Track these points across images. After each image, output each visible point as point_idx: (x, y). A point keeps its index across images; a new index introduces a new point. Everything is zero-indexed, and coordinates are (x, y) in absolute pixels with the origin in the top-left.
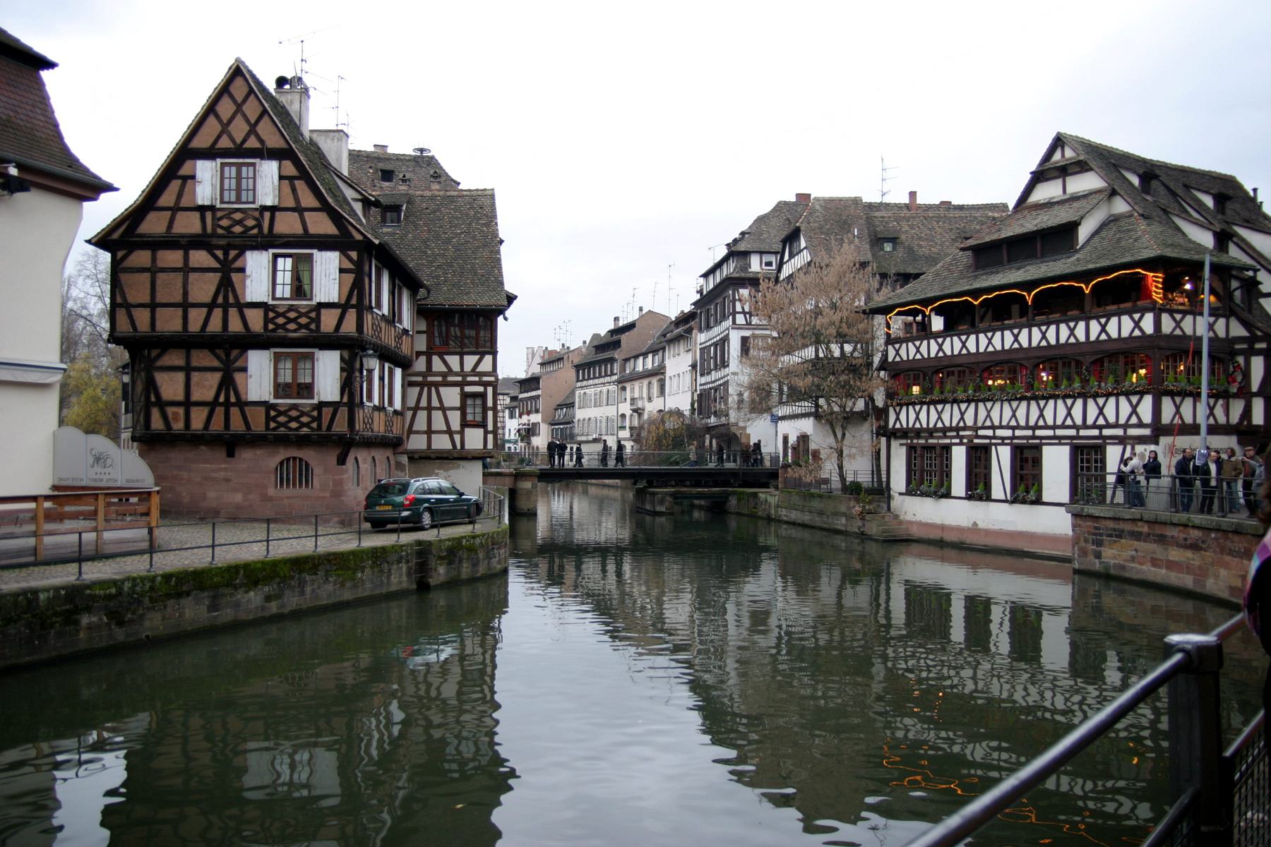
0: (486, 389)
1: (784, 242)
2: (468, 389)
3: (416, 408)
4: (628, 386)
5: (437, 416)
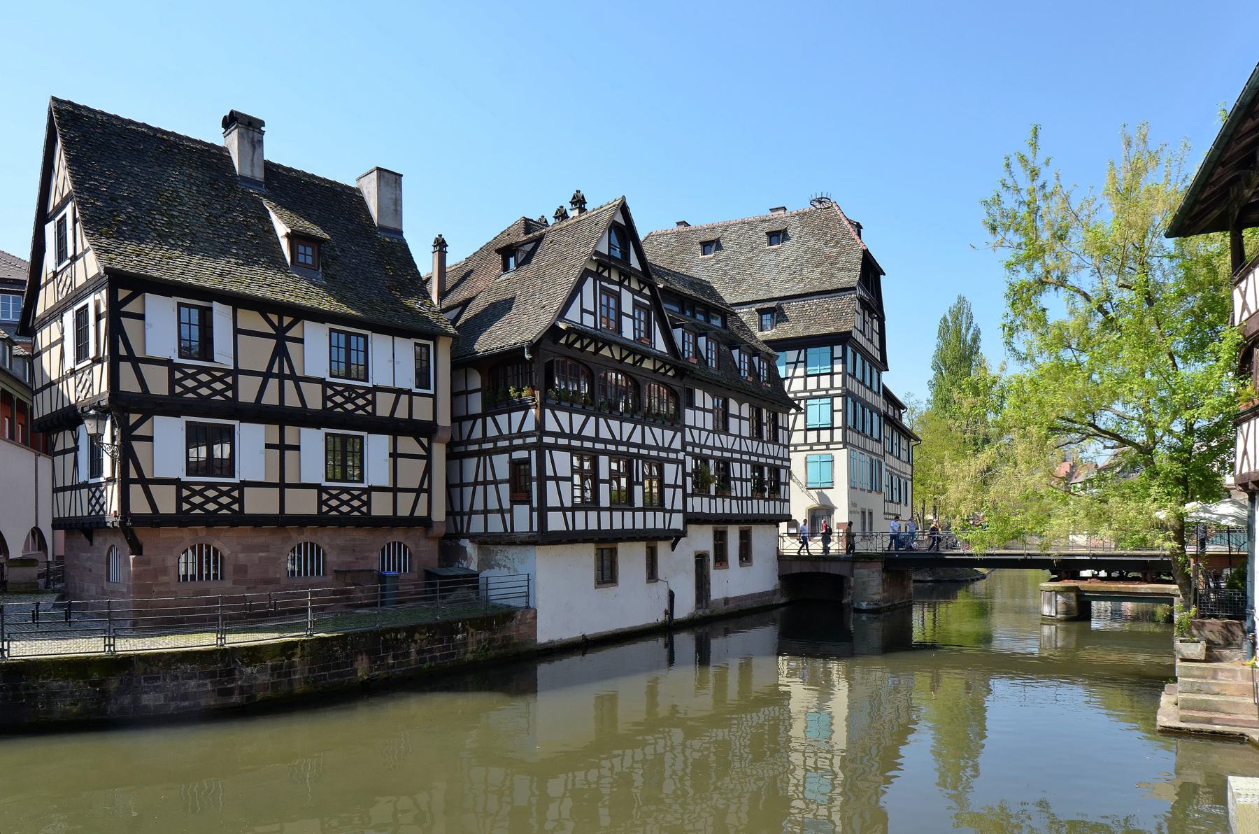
2: (517, 455)
3: (476, 483)
5: (491, 488)
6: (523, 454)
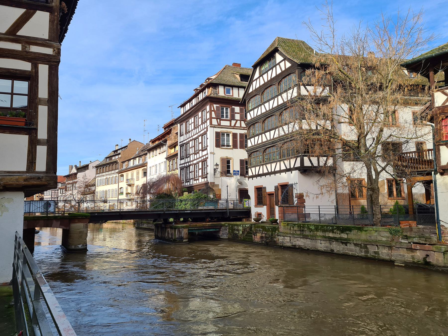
0: (35, 67)
1: (255, 67)
4: (125, 174)
6: (26, 66)
